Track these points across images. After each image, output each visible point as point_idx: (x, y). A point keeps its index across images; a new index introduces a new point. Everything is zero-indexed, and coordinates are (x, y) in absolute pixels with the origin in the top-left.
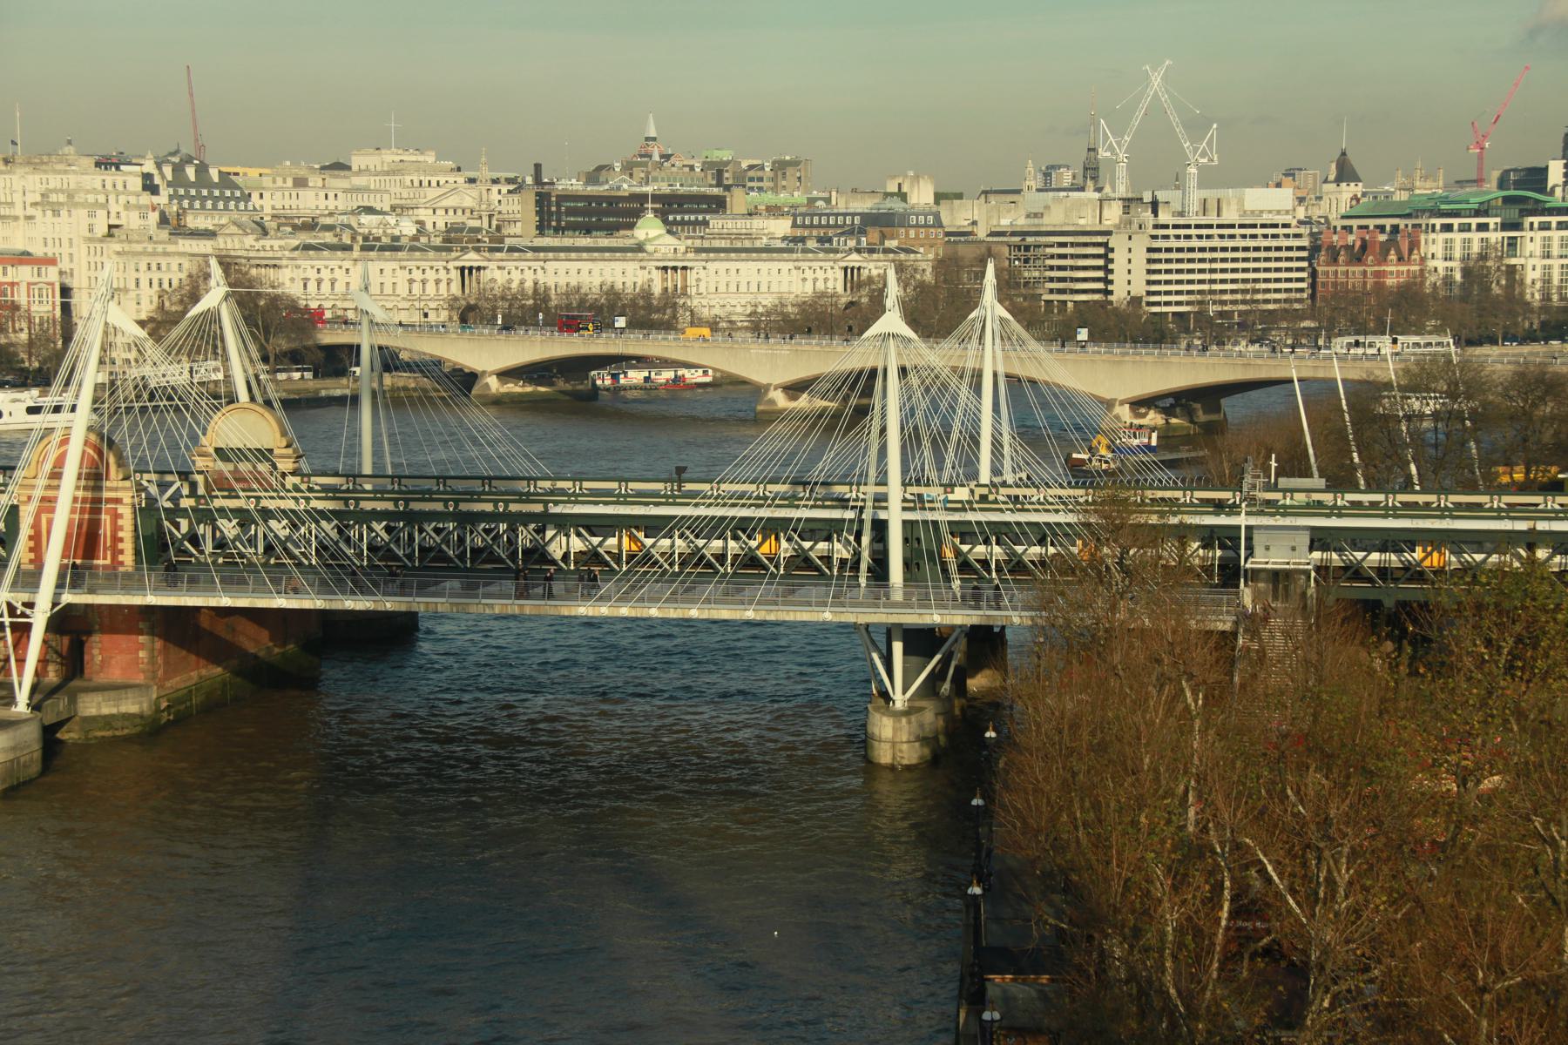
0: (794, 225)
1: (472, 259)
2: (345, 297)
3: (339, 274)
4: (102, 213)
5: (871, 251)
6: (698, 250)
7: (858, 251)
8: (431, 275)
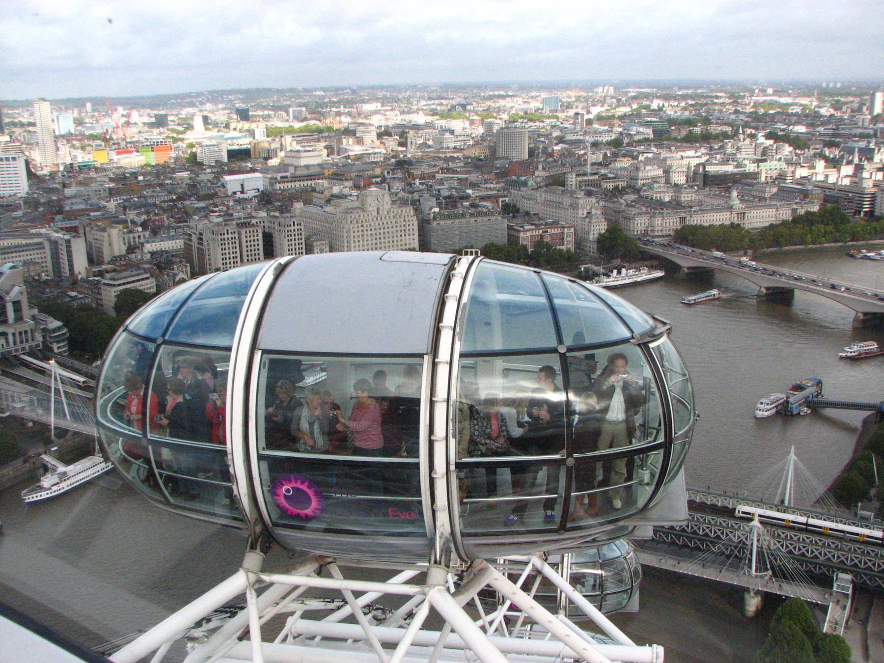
0: (779, 189)
1: (683, 215)
2: (647, 227)
3: (646, 221)
4: (585, 210)
5: (800, 203)
6: (748, 207)
7: (796, 203)
8: (672, 220)
